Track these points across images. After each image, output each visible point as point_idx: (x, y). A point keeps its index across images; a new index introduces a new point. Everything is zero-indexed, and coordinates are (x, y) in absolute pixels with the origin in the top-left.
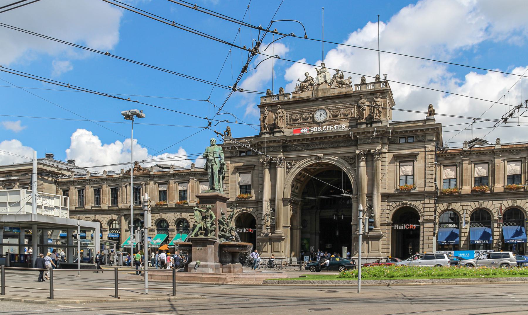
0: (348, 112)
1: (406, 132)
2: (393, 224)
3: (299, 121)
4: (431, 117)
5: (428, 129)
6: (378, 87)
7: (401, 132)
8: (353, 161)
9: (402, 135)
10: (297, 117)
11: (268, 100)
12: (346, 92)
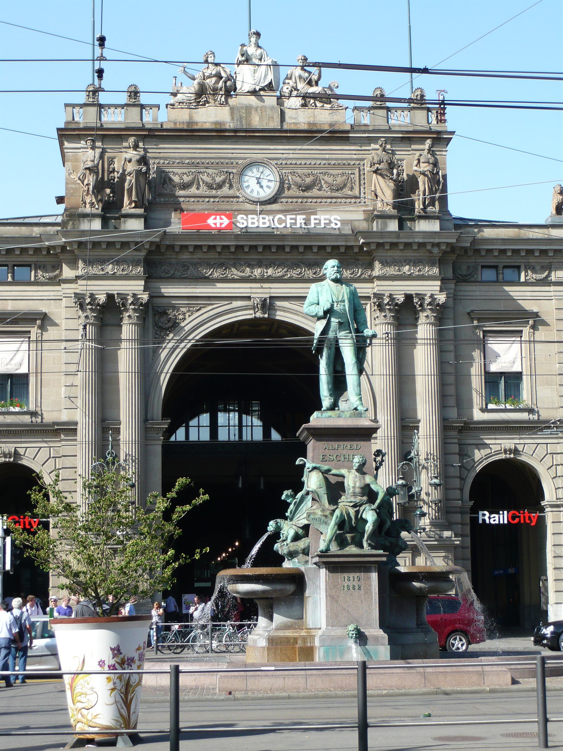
0: (340, 180)
1: (503, 252)
2: (475, 510)
7: (489, 251)
9: (490, 261)
10: (186, 179)
12: (331, 125)
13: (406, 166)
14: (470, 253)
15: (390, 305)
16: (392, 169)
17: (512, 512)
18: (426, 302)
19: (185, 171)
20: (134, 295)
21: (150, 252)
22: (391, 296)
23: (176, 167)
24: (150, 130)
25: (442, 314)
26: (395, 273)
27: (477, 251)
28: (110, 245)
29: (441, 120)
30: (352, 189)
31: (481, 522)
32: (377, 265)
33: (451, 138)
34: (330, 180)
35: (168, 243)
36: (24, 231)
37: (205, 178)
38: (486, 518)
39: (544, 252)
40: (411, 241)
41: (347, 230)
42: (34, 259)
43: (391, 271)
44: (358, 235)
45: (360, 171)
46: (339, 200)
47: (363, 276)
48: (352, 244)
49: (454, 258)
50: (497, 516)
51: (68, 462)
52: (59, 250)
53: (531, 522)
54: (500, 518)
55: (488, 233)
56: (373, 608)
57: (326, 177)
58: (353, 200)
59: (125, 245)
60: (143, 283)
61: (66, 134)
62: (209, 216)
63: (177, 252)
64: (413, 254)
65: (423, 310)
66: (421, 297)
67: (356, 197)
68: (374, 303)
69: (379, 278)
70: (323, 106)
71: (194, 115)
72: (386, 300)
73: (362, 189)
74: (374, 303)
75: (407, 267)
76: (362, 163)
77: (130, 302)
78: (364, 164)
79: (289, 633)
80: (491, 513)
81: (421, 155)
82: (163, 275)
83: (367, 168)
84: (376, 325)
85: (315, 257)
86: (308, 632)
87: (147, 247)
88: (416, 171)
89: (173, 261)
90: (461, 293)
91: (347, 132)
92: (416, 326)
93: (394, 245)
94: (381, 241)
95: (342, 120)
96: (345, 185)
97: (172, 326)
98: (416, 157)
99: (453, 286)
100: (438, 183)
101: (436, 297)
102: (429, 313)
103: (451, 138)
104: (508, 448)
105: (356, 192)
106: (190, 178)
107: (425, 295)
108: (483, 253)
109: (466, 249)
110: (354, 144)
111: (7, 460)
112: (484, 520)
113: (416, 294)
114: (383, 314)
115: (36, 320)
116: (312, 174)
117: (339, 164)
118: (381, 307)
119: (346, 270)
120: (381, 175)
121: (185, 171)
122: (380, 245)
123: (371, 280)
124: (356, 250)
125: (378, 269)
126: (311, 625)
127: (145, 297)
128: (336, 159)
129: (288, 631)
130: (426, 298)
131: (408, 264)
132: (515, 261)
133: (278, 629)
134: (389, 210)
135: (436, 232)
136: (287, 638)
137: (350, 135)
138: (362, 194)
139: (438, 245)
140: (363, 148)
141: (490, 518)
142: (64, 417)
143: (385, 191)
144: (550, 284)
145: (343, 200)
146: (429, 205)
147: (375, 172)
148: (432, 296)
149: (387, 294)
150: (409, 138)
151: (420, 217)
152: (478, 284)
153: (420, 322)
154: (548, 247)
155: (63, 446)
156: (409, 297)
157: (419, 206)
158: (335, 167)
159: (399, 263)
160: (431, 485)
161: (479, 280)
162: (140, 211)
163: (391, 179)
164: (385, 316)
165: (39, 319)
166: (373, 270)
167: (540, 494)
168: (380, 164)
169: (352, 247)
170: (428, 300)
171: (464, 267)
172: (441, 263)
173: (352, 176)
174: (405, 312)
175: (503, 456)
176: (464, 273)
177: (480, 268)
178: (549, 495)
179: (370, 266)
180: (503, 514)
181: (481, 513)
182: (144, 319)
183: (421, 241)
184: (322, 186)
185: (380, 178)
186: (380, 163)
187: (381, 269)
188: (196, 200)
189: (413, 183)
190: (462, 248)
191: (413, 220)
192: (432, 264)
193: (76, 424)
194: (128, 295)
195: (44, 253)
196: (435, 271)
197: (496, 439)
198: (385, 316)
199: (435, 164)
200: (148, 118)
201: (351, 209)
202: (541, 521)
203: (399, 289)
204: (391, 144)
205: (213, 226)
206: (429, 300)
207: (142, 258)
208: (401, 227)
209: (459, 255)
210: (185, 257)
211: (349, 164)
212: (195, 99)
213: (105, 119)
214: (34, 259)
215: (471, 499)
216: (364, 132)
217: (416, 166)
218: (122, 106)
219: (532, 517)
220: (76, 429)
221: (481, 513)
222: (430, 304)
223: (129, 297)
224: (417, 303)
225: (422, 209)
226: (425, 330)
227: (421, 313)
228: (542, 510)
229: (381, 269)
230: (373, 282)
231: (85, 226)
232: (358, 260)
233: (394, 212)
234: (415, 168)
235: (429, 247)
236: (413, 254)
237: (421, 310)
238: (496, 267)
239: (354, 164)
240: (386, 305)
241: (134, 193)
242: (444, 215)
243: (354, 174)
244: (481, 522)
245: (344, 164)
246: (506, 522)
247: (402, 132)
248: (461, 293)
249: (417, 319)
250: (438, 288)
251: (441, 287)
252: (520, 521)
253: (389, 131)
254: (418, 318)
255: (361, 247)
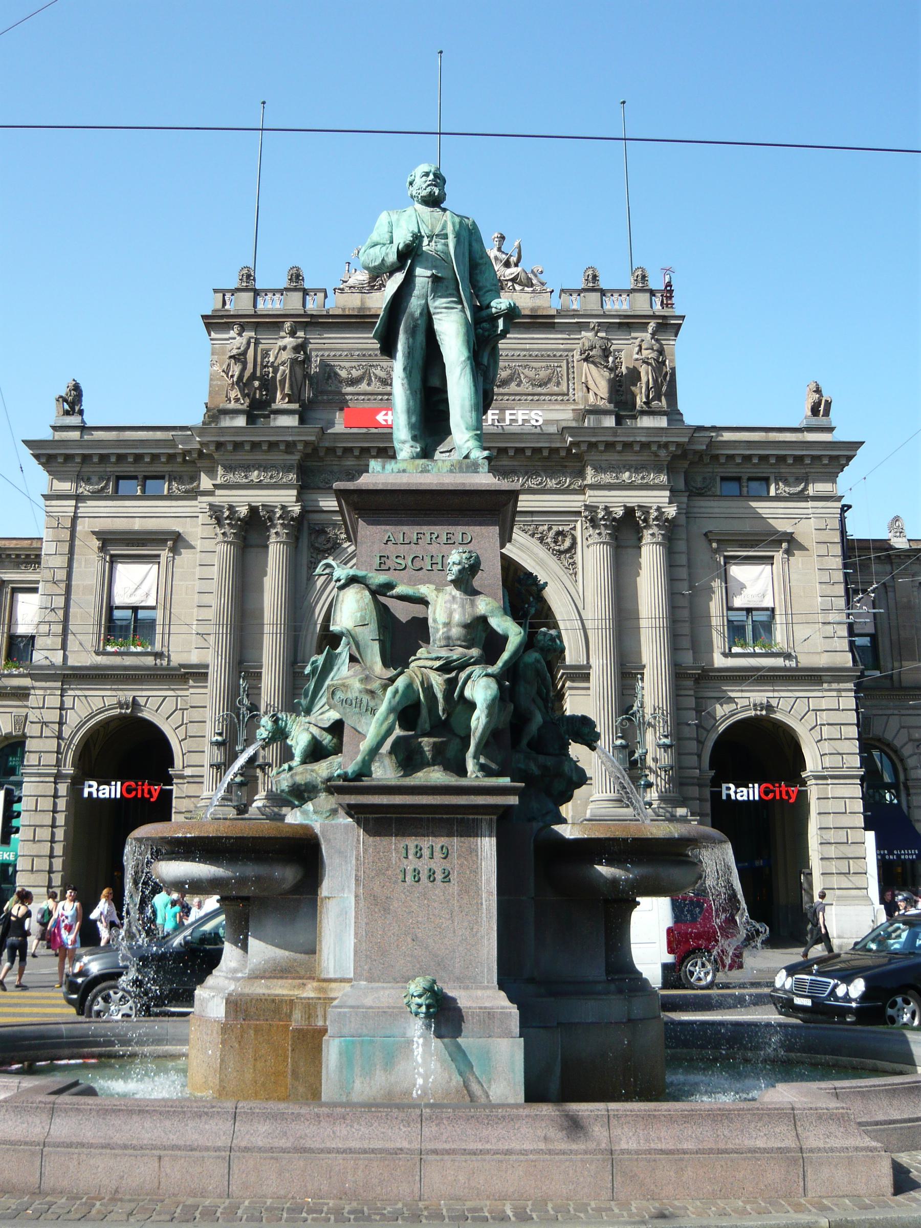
0: (543, 374)
2: (717, 782)
3: (363, 387)
4: (821, 421)
5: (819, 458)
6: (641, 304)
7: (731, 457)
8: (567, 544)
9: (732, 471)
10: (355, 373)
11: (241, 304)
12: (532, 309)
13: (626, 358)
14: (707, 460)
15: (605, 520)
16: (607, 357)
17: (764, 785)
18: (652, 517)
19: (353, 364)
20: (283, 508)
21: (306, 457)
22: (606, 508)
23: (343, 360)
24: (312, 316)
25: (672, 533)
26: (612, 481)
27: (715, 458)
28: (255, 445)
29: (667, 305)
30: (558, 384)
31: (724, 797)
32: (589, 471)
33: (681, 324)
34: (531, 374)
35: (327, 445)
36: (159, 435)
37: (378, 372)
38: (732, 792)
39: (799, 459)
40: (631, 439)
41: (553, 429)
42: (168, 468)
43: (607, 478)
44: (565, 431)
45: (568, 363)
46: (542, 398)
47: (572, 487)
48: (558, 445)
49: (686, 466)
50: (745, 790)
51: (196, 715)
52: (195, 455)
53: (790, 798)
54: (750, 793)
55: (727, 436)
56: (483, 930)
57: (526, 371)
58: (560, 398)
59: (273, 445)
60: (295, 492)
61: (214, 322)
62: (378, 411)
63: (339, 457)
64: (635, 458)
65: (648, 526)
66: (645, 510)
67: (563, 395)
68: (586, 517)
69: (592, 487)
70: (523, 290)
71: (367, 300)
72: (601, 514)
73: (571, 385)
74: (586, 517)
75: (627, 474)
76: (570, 354)
77: (278, 515)
78: (573, 356)
79: (281, 989)
80: (737, 787)
81: (643, 341)
82: (321, 485)
83: (577, 356)
84: (588, 547)
85: (510, 463)
86: (321, 990)
87: (300, 447)
88: (637, 360)
89: (336, 468)
90: (696, 510)
91: (553, 317)
92: (640, 548)
93: (610, 446)
94: (594, 439)
95: (546, 305)
96: (550, 380)
97: (332, 548)
98: (637, 342)
99: (685, 499)
100: (666, 385)
101: (663, 510)
102: (655, 530)
103: (681, 324)
104: (758, 702)
105: (564, 388)
106: (360, 372)
107: (651, 508)
108: (723, 460)
109: (700, 455)
110: (562, 332)
111: (123, 711)
112: (729, 796)
113: (639, 506)
114: (598, 531)
115: (166, 540)
116: (510, 368)
117: (542, 356)
118: (594, 523)
119: (551, 480)
120: (594, 363)
121: (353, 364)
122: (592, 445)
123: (581, 491)
124: (563, 453)
125: (590, 476)
126: (331, 970)
127: (296, 509)
128: (539, 350)
129: (280, 982)
130: (651, 511)
131: (628, 470)
132: (763, 471)
133: (255, 976)
134: (603, 404)
135: (662, 429)
136: (273, 1001)
137: (556, 321)
138: (571, 390)
139: (666, 445)
140: (572, 336)
141: (736, 793)
142: (194, 658)
143: (598, 383)
144: (807, 498)
145: (547, 398)
146: (653, 400)
147: (586, 360)
148: (659, 509)
149: (601, 506)
150: (629, 324)
151: (643, 413)
152: (716, 498)
153: (644, 542)
154: (804, 453)
155: (193, 693)
156: (629, 512)
157: (640, 401)
158: (537, 358)
159: (617, 468)
160: (659, 746)
161: (719, 493)
162: (295, 406)
163: (606, 367)
164: (599, 534)
165: (170, 540)
166: (584, 479)
167: (800, 762)
168: (591, 350)
169: (557, 450)
170: (653, 514)
171: (699, 478)
172: (671, 470)
173: (559, 369)
174: (624, 531)
175: (752, 713)
176: (699, 485)
177: (718, 479)
178: (812, 762)
179: (581, 474)
180: (754, 787)
181: (724, 786)
182: (297, 539)
183: (643, 439)
184: (521, 381)
185: (592, 366)
186: (592, 348)
187: (594, 476)
188: (366, 397)
189: (634, 375)
190: (696, 452)
191: (634, 417)
192: (659, 471)
193: (207, 666)
194: (276, 507)
195: (179, 460)
196: (663, 478)
197: (742, 691)
198: (599, 534)
199: (661, 352)
200: (313, 305)
201: (558, 407)
202: (803, 797)
203: (617, 501)
204: (606, 332)
205: (384, 423)
206: (656, 514)
207: (295, 463)
208: (619, 421)
209: (691, 464)
210: (349, 463)
211: (555, 356)
212: (369, 283)
213: (260, 306)
214: (168, 468)
215: (711, 768)
216: (573, 316)
217: (637, 353)
218: (281, 291)
219: (791, 793)
220: (207, 673)
221: (724, 786)
222: (656, 519)
223: (277, 510)
224: (640, 518)
225: (645, 403)
226: (650, 557)
227: (645, 531)
228: (803, 783)
229: (594, 476)
230: (585, 494)
231: (226, 422)
232: (566, 467)
233: (611, 407)
234: (636, 356)
235: (654, 448)
236: (635, 458)
237: (645, 527)
238: (738, 479)
239: (561, 356)
240: (601, 519)
241: (287, 385)
242: (673, 414)
243: (560, 367)
244: (724, 797)
245: (549, 356)
246: (757, 798)
247: (619, 316)
248: (696, 510)
249: (640, 539)
250: (667, 500)
251: (670, 497)
252: (775, 796)
253: (605, 316)
254: (642, 537)
255: (569, 450)
